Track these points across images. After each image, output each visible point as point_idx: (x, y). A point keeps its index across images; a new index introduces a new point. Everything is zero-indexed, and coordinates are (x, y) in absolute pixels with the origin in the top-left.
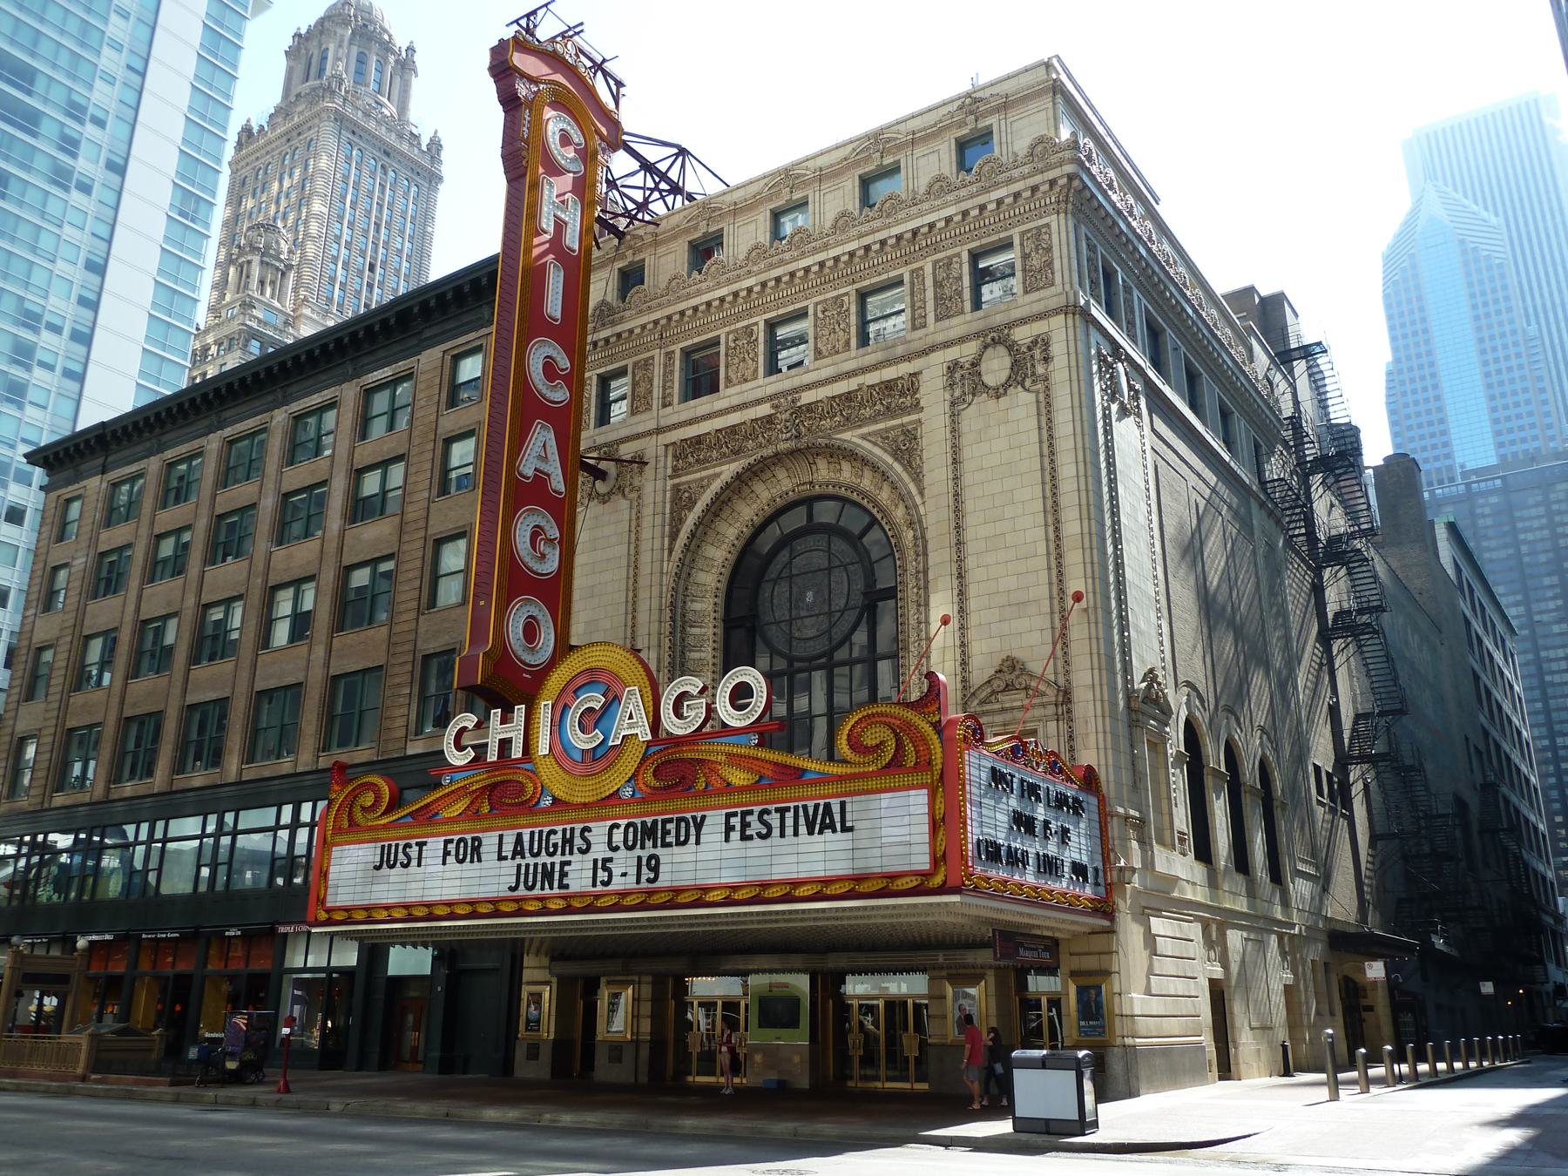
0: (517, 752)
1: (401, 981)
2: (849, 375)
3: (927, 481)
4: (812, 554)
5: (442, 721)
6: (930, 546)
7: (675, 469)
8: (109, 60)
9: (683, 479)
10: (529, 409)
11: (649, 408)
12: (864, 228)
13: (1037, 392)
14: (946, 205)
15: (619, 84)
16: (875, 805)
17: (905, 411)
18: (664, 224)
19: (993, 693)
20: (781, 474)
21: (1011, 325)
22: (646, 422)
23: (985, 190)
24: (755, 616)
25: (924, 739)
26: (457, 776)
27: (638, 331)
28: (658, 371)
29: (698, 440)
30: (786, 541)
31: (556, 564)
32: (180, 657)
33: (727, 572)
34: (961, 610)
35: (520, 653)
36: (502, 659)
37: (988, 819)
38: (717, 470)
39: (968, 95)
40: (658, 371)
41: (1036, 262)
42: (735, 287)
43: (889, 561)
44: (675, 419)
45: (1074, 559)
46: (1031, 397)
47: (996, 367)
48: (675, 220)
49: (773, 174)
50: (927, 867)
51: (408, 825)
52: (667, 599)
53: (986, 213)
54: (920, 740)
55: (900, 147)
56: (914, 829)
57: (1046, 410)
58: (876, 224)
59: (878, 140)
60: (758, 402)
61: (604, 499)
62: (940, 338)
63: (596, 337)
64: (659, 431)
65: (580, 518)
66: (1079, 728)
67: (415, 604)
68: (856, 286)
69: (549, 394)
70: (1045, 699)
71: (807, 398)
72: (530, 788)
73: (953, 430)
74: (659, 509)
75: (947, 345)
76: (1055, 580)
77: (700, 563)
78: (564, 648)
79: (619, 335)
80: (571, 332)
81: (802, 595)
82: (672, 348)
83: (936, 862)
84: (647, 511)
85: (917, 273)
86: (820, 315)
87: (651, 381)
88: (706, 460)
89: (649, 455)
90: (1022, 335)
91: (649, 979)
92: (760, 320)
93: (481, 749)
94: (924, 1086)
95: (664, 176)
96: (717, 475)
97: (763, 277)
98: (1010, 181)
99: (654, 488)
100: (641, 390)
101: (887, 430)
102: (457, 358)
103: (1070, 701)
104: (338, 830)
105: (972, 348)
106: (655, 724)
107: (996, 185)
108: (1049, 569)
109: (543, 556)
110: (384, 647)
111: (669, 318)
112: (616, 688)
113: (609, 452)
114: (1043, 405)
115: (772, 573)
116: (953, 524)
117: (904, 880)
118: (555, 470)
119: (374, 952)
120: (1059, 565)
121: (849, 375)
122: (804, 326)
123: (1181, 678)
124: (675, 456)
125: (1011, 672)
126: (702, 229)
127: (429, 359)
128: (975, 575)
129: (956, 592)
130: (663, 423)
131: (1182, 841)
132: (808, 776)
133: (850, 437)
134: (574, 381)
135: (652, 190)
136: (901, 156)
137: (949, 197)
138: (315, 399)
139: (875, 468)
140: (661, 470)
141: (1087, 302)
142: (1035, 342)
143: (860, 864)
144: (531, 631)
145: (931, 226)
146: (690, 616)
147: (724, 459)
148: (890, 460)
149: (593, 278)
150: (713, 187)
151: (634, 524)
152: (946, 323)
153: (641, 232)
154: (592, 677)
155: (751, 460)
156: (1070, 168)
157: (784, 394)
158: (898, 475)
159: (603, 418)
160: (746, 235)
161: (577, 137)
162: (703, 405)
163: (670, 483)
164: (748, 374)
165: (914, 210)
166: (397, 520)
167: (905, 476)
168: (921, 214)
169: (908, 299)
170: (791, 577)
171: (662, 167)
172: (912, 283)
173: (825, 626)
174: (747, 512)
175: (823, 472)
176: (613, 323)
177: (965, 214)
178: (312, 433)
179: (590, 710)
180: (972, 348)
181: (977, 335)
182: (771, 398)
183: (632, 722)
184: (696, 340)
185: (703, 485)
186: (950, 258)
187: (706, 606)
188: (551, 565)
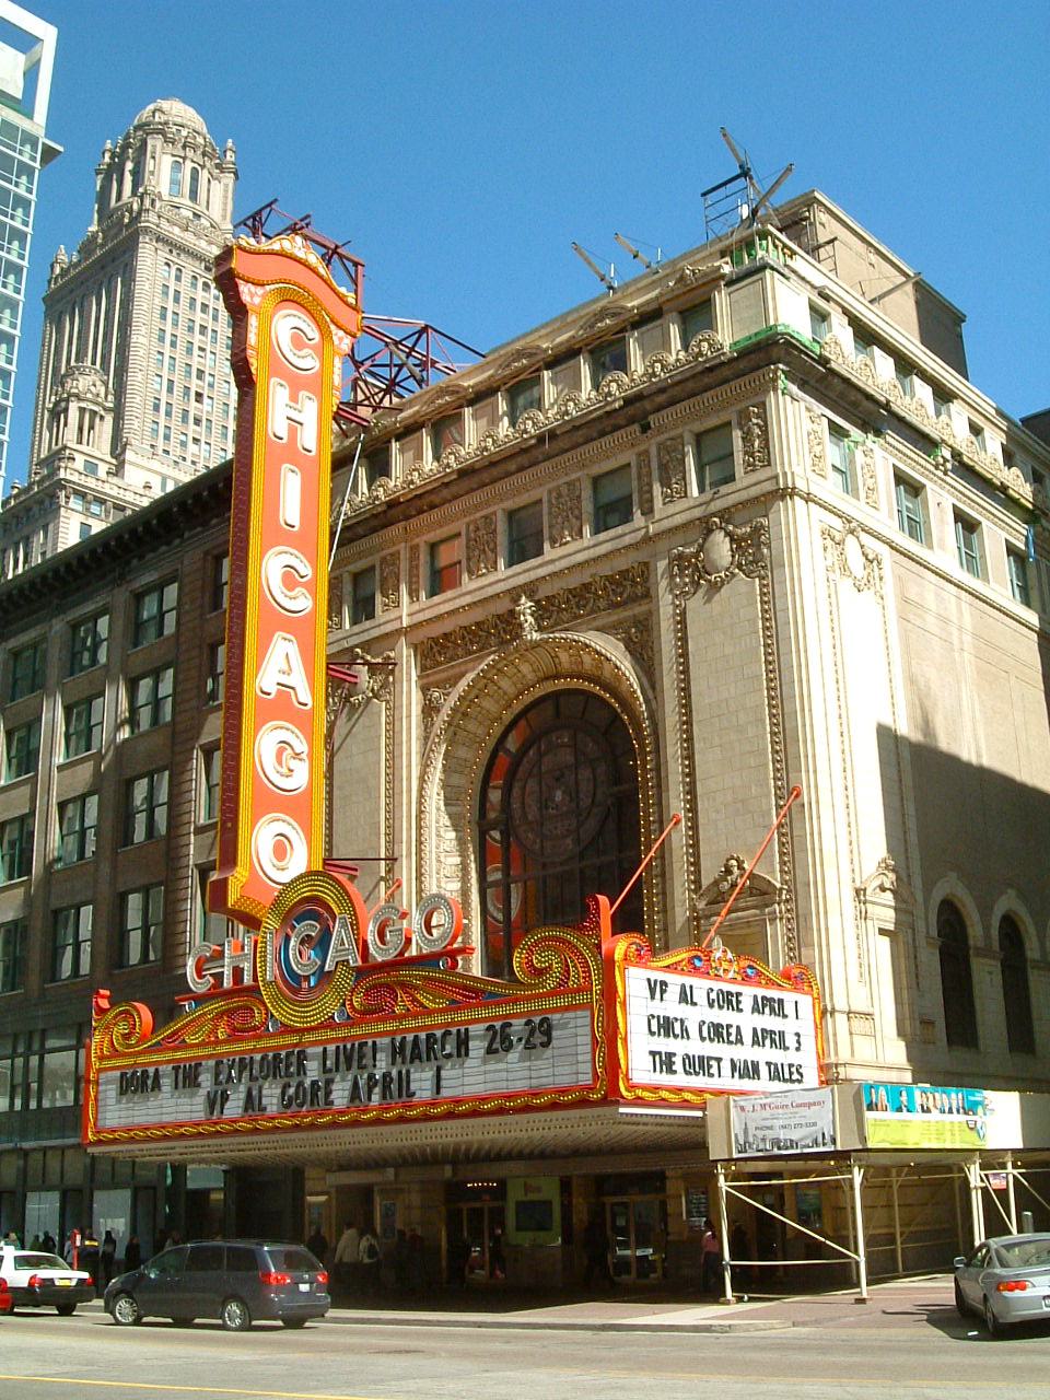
0: (247, 980)
15: (356, 264)
17: (634, 599)
28: (404, 565)
40: (404, 565)
72: (258, 1018)
82: (417, 541)
93: (219, 977)
118: (298, 679)
143: (534, 1082)
161: (313, 332)
166: (170, 729)
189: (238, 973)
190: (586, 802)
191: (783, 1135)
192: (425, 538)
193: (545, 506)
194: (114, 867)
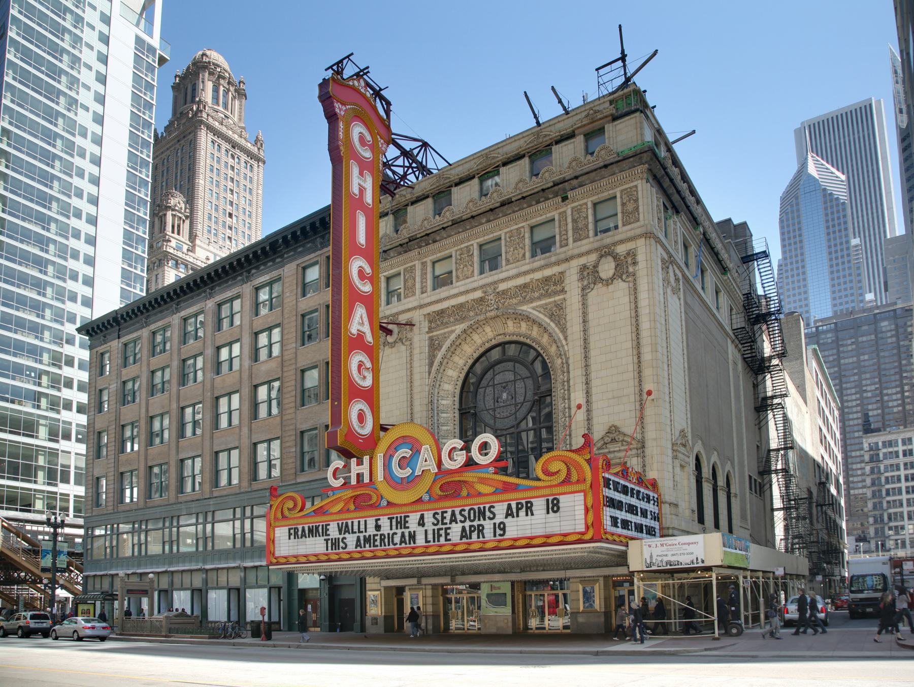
3: (569, 332)
6: (571, 368)
9: (435, 333)
11: (414, 294)
17: (556, 293)
28: (418, 273)
30: (492, 366)
33: (460, 383)
34: (588, 402)
38: (453, 328)
40: (418, 273)
44: (428, 300)
45: (647, 372)
60: (475, 290)
61: (392, 345)
64: (421, 307)
70: (631, 446)
71: (502, 287)
77: (445, 379)
81: (500, 397)
84: (416, 351)
88: (447, 323)
96: (453, 331)
99: (420, 339)
100: (410, 283)
101: (546, 304)
102: (304, 269)
116: (583, 356)
120: (640, 376)
125: (614, 434)
127: (289, 270)
128: (594, 383)
130: (422, 302)
133: (526, 308)
135: (408, 168)
138: (229, 294)
139: (540, 325)
146: (441, 407)
148: (548, 320)
150: (442, 164)
151: (409, 359)
154: (404, 440)
162: (444, 292)
163: (427, 336)
167: (556, 329)
170: (494, 385)
182: (482, 287)
185: (445, 337)
187: (449, 402)
190: (520, 399)
191: (673, 559)
192: (431, 258)
193: (503, 242)
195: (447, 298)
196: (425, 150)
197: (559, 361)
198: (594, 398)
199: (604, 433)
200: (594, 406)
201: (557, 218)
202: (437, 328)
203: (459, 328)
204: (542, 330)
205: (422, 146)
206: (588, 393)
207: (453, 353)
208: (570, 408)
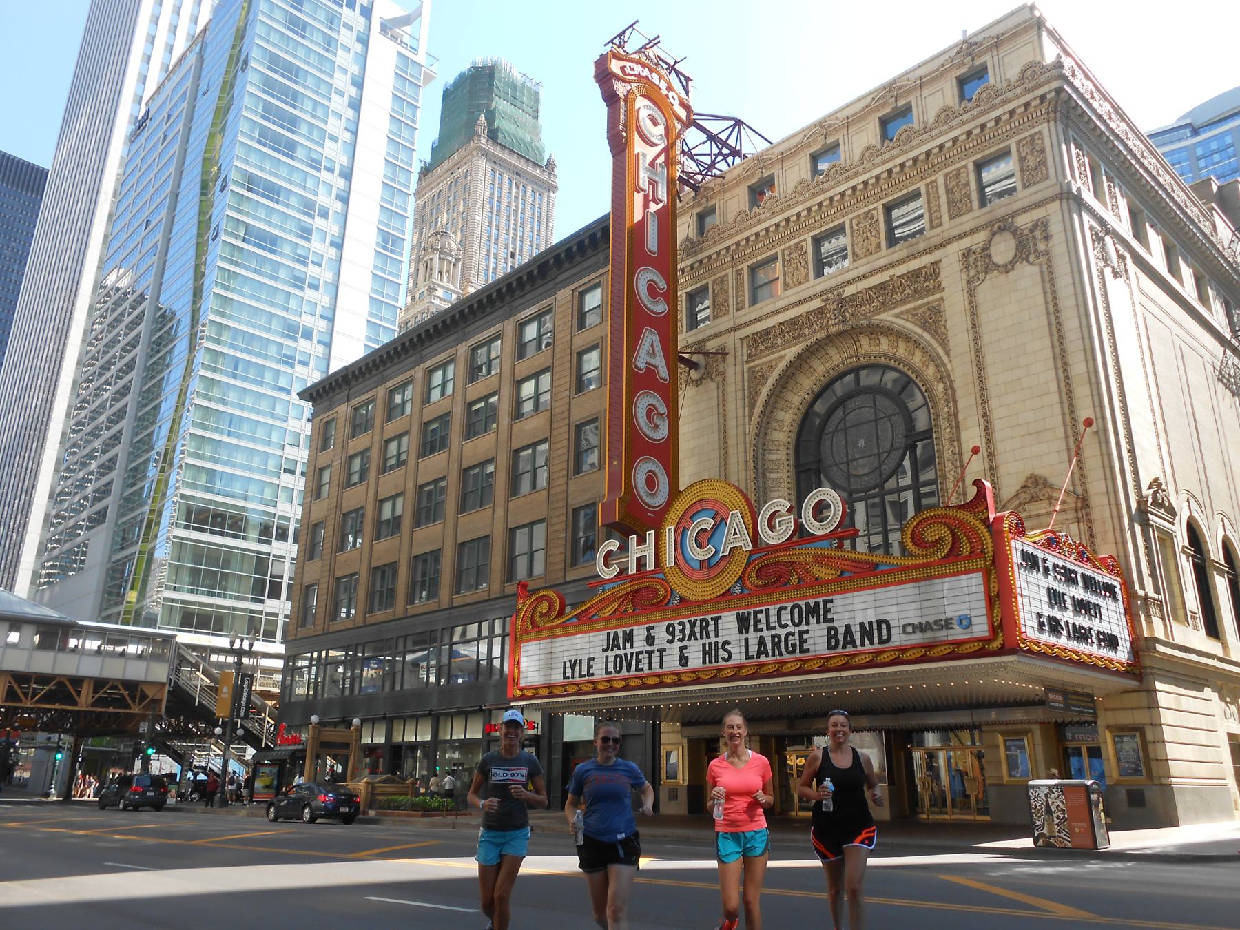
0: (650, 566)
1: (571, 747)
2: (882, 269)
3: (952, 344)
4: (861, 410)
5: (591, 547)
6: (958, 395)
7: (750, 356)
8: (342, 58)
10: (638, 319)
12: (886, 156)
13: (1041, 265)
14: (952, 129)
15: (688, 79)
16: (938, 587)
17: (929, 292)
18: (728, 177)
19: (1021, 504)
20: (832, 351)
21: (1013, 215)
22: (725, 323)
23: (984, 112)
24: (819, 461)
25: (975, 530)
26: (607, 587)
27: (714, 257)
29: (766, 332)
30: (841, 402)
31: (666, 432)
32: (407, 523)
33: (795, 430)
35: (644, 497)
36: (631, 503)
37: (1031, 595)
38: (783, 353)
39: (965, 42)
41: (1031, 162)
42: (786, 215)
43: (924, 409)
46: (1036, 269)
47: (1003, 250)
48: (737, 172)
49: (810, 128)
50: (986, 634)
51: (575, 625)
52: (750, 453)
53: (987, 131)
54: (972, 534)
55: (910, 91)
56: (973, 605)
57: (1049, 279)
58: (895, 152)
59: (892, 89)
60: (811, 298)
61: (697, 383)
62: (955, 232)
63: (683, 265)
64: (735, 329)
65: (680, 400)
66: (1097, 528)
67: (564, 472)
68: (883, 201)
69: (652, 308)
71: (849, 291)
73: (971, 302)
74: (739, 387)
75: (961, 237)
76: (1067, 411)
77: (774, 424)
78: (674, 493)
79: (700, 262)
80: (666, 261)
83: (994, 630)
84: (731, 389)
85: (932, 185)
86: (855, 227)
87: (727, 293)
88: (773, 347)
89: (729, 347)
90: (1023, 221)
91: (758, 738)
92: (808, 237)
94: (988, 818)
95: (725, 144)
96: (782, 357)
97: (808, 204)
98: (1006, 101)
99: (734, 372)
100: (720, 300)
101: (915, 308)
102: (582, 295)
103: (1088, 506)
104: (525, 631)
105: (982, 236)
106: (755, 538)
107: (994, 107)
108: (1061, 402)
109: (657, 426)
110: (545, 504)
111: (738, 244)
112: (723, 513)
113: (699, 348)
114: (1046, 273)
115: (830, 427)
116: (976, 375)
117: (968, 646)
119: (553, 722)
121: (882, 269)
122: (844, 240)
123: (1180, 487)
124: (749, 346)
125: (1036, 487)
126: (758, 176)
127: (564, 295)
128: (997, 413)
129: (982, 428)
130: (739, 322)
131: (1194, 618)
132: (881, 568)
133: (886, 317)
134: (670, 297)
135: (716, 155)
136: (912, 98)
137: (954, 122)
138: (486, 334)
140: (739, 358)
141: (1079, 189)
142: (1035, 227)
144: (651, 482)
145: (941, 147)
146: (769, 465)
147: (786, 344)
148: (920, 331)
149: (679, 222)
152: (959, 220)
153: (712, 185)
155: (808, 343)
156: (1055, 84)
157: (831, 290)
158: (928, 342)
159: (693, 323)
160: (794, 174)
163: (746, 367)
164: (801, 278)
165: (926, 136)
166: (548, 414)
167: (933, 342)
168: (932, 138)
169: (926, 206)
170: (846, 429)
171: (723, 136)
172: (928, 194)
173: (876, 464)
174: (808, 383)
175: (866, 346)
176: (695, 253)
177: (969, 133)
178: (485, 359)
179: (704, 530)
180: (982, 236)
181: (985, 226)
182: (820, 294)
183: (735, 536)
184: (759, 258)
186: (958, 170)
187: (781, 458)
188: (662, 433)
189: (640, 562)
194: (507, 511)
195: (773, 314)
196: (739, 131)
197: (941, 385)
198: (998, 436)
199: (1019, 487)
200: (1000, 448)
201: (923, 191)
202: (759, 355)
203: (791, 353)
204: (911, 345)
205: (734, 126)
206: (988, 430)
207: (784, 387)
208: (961, 454)
